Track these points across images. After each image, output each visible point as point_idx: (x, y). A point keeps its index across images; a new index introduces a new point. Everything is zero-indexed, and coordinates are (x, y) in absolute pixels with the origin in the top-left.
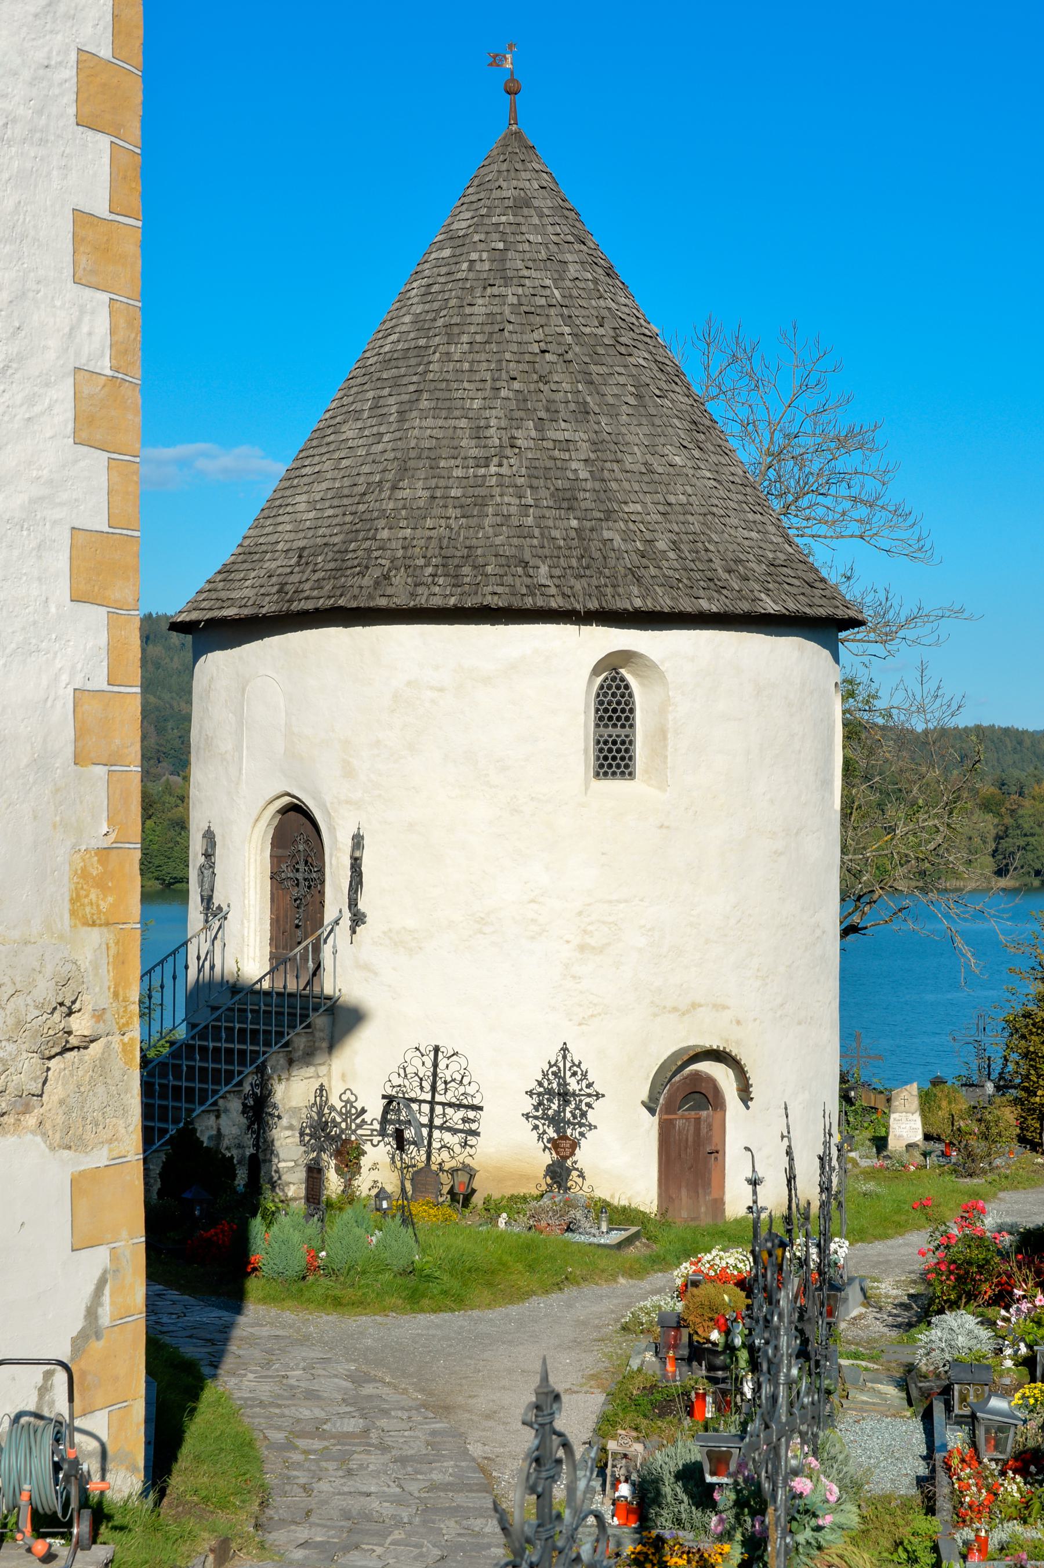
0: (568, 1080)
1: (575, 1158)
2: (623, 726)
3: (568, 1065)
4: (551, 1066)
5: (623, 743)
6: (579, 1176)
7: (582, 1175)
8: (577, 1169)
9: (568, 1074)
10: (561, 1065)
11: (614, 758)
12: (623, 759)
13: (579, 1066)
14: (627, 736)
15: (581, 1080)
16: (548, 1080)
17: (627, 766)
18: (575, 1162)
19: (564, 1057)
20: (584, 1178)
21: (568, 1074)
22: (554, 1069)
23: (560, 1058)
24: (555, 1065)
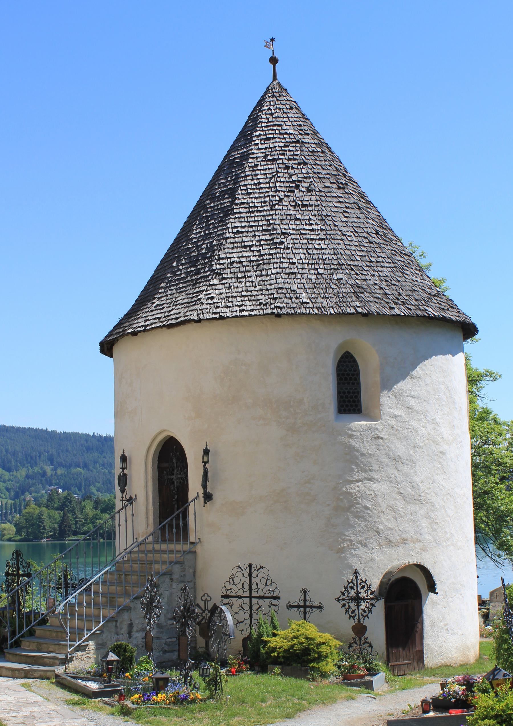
0: (360, 591)
1: (366, 635)
2: (353, 384)
3: (359, 582)
4: (349, 583)
5: (354, 393)
6: (369, 646)
7: (371, 646)
8: (368, 643)
9: (359, 587)
10: (355, 582)
11: (349, 401)
12: (354, 402)
13: (365, 582)
14: (356, 389)
15: (367, 590)
16: (348, 591)
17: (356, 406)
18: (367, 638)
19: (357, 578)
20: (372, 647)
21: (359, 587)
22: (351, 585)
23: (354, 578)
24: (351, 582)
